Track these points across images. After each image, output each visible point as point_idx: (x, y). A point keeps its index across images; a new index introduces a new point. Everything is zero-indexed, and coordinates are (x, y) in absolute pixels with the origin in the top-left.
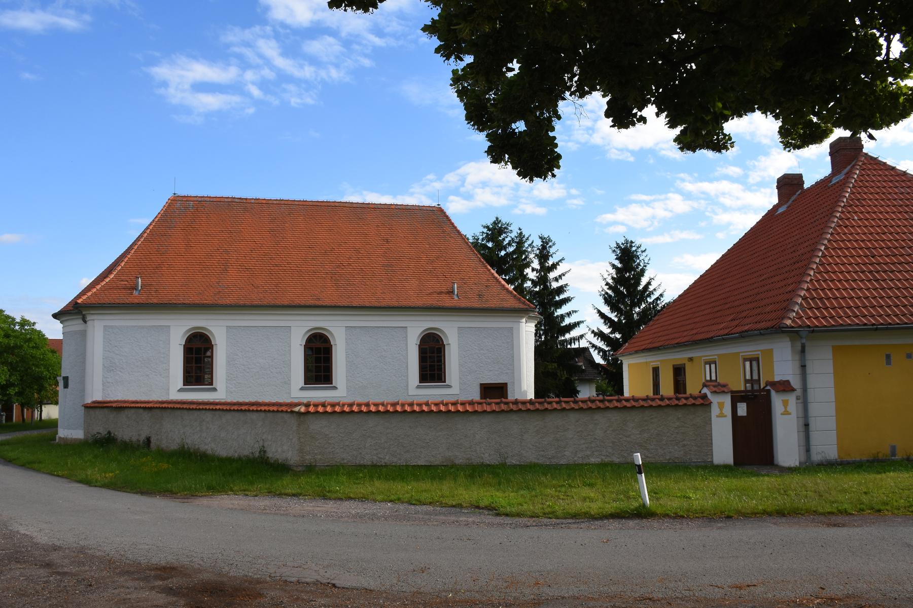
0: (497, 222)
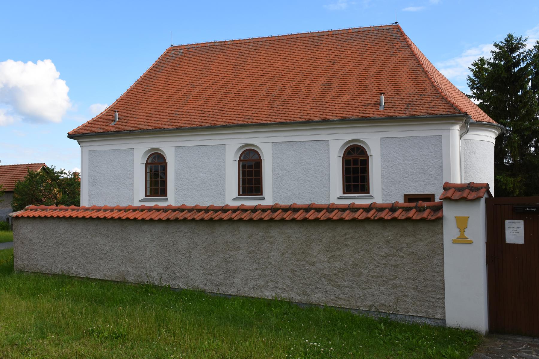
0: (509, 39)
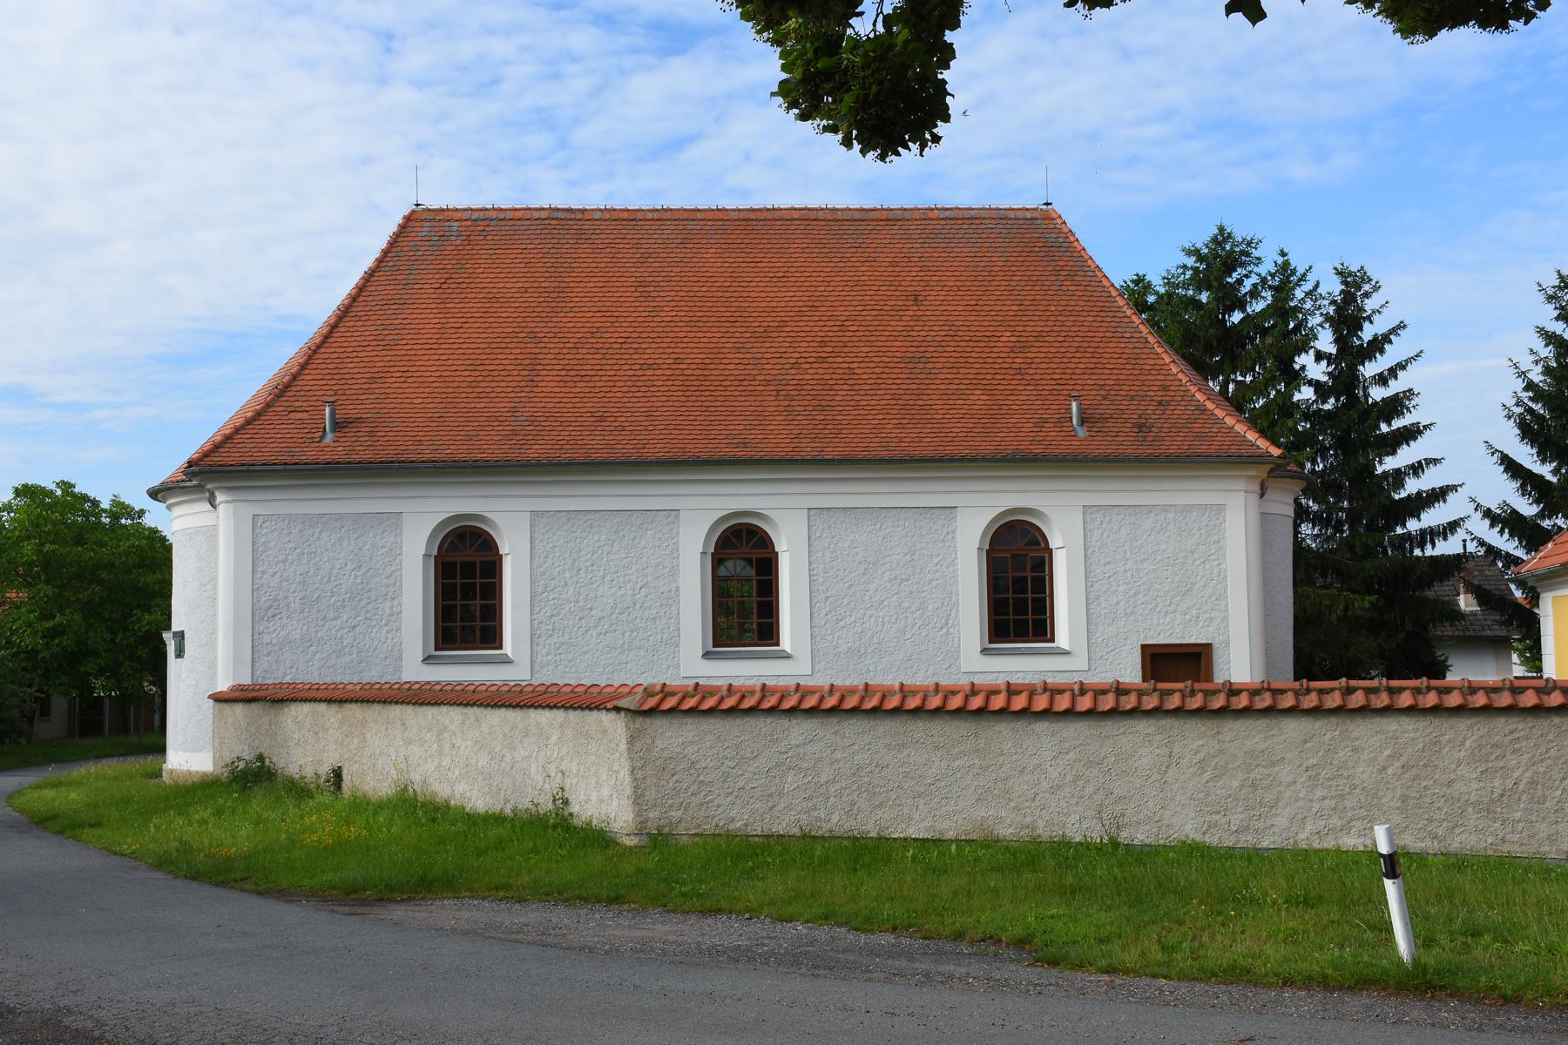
0: (1222, 236)
